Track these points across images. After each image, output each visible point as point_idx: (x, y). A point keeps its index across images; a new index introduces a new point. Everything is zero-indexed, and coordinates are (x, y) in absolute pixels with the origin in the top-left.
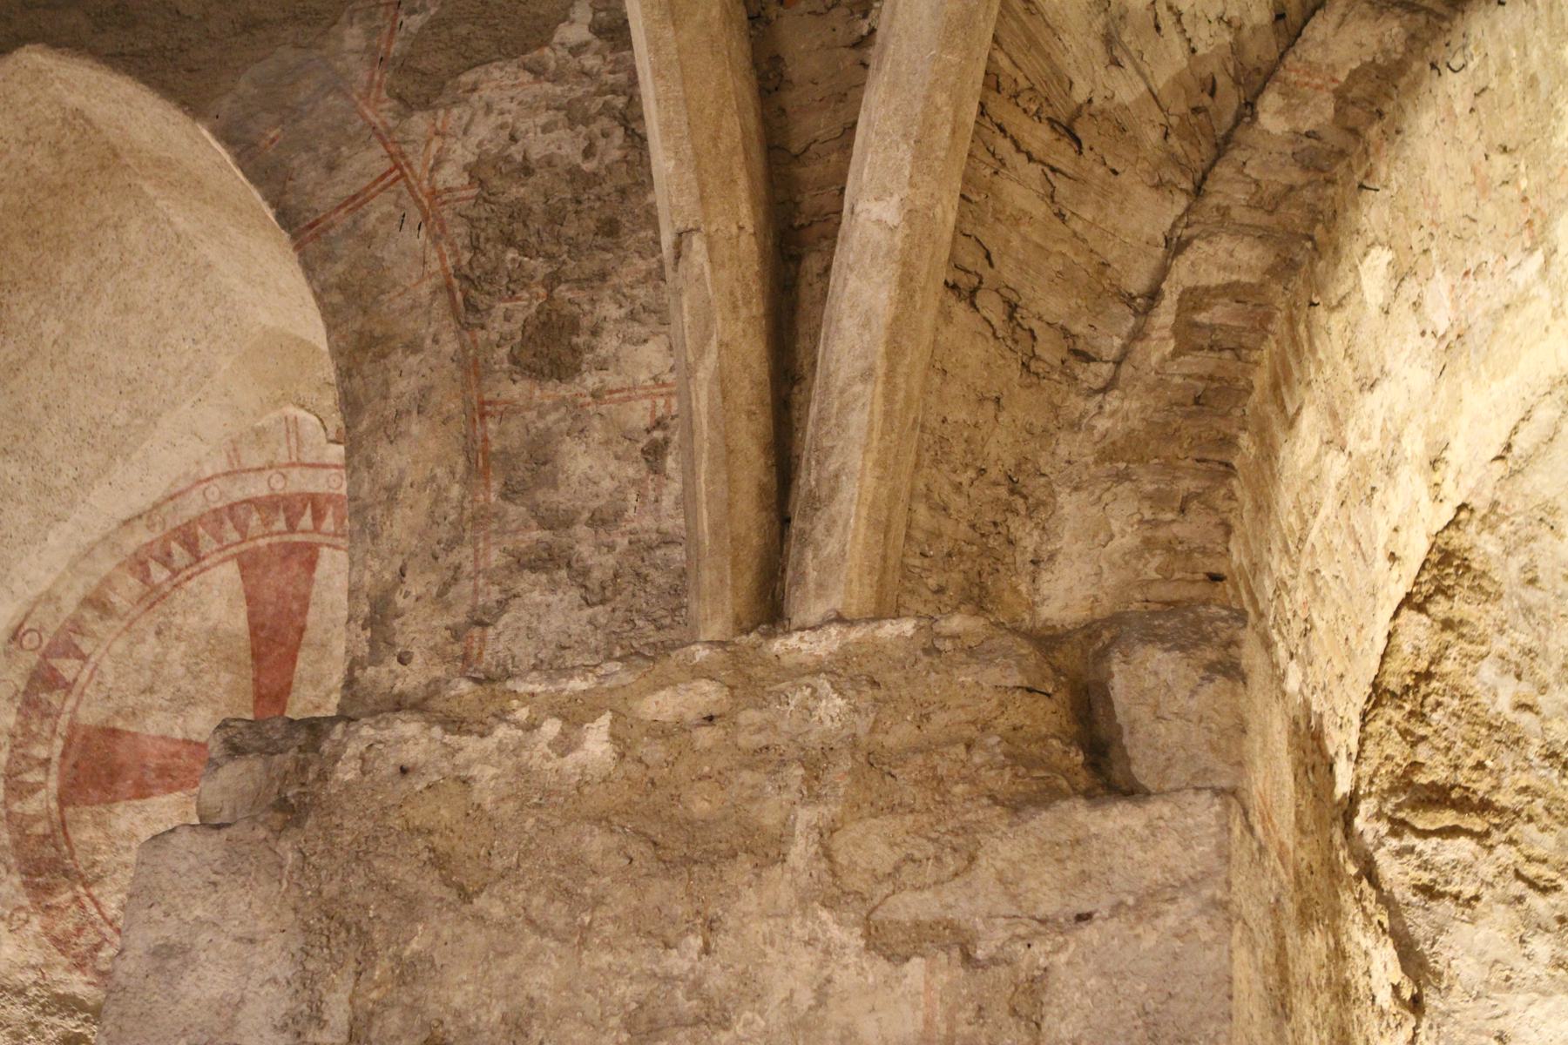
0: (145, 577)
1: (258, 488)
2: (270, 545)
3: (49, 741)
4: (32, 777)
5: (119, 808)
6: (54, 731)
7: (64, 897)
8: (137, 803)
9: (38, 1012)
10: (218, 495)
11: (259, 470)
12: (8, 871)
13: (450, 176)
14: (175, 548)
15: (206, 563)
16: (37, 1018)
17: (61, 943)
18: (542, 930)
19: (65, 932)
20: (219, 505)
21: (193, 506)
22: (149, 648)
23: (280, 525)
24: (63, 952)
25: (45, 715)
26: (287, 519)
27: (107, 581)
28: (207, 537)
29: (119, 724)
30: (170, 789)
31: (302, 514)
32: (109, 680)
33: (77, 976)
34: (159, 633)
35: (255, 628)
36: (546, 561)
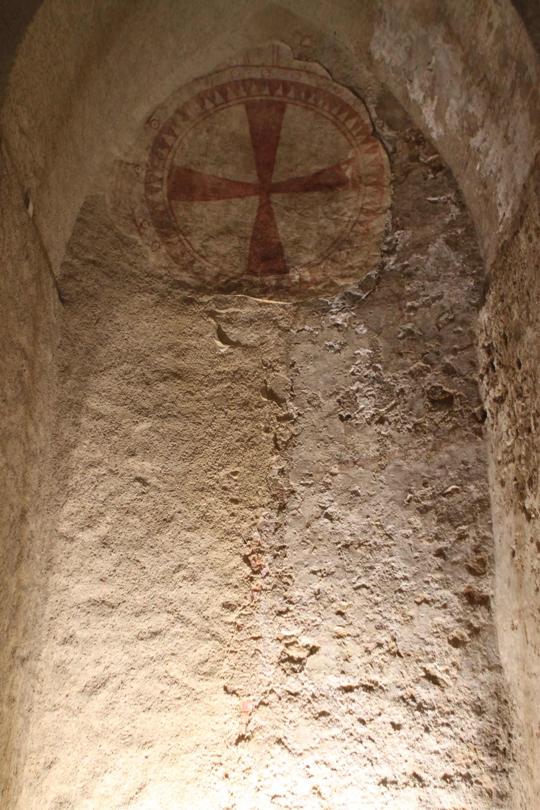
0: (203, 105)
1: (256, 74)
2: (261, 100)
3: (162, 171)
4: (156, 185)
5: (195, 204)
6: (164, 167)
7: (175, 239)
8: (203, 202)
9: (170, 287)
11: (258, 67)
12: (149, 225)
14: (217, 94)
15: (230, 103)
16: (170, 290)
17: (176, 259)
19: (176, 254)
20: (238, 79)
21: (226, 78)
22: (204, 137)
23: (266, 91)
24: (177, 263)
25: (160, 159)
26: (270, 90)
27: (186, 104)
28: (231, 92)
29: (193, 168)
30: (219, 199)
31: (278, 88)
32: (187, 147)
33: (184, 273)
34: (208, 131)
35: (253, 134)
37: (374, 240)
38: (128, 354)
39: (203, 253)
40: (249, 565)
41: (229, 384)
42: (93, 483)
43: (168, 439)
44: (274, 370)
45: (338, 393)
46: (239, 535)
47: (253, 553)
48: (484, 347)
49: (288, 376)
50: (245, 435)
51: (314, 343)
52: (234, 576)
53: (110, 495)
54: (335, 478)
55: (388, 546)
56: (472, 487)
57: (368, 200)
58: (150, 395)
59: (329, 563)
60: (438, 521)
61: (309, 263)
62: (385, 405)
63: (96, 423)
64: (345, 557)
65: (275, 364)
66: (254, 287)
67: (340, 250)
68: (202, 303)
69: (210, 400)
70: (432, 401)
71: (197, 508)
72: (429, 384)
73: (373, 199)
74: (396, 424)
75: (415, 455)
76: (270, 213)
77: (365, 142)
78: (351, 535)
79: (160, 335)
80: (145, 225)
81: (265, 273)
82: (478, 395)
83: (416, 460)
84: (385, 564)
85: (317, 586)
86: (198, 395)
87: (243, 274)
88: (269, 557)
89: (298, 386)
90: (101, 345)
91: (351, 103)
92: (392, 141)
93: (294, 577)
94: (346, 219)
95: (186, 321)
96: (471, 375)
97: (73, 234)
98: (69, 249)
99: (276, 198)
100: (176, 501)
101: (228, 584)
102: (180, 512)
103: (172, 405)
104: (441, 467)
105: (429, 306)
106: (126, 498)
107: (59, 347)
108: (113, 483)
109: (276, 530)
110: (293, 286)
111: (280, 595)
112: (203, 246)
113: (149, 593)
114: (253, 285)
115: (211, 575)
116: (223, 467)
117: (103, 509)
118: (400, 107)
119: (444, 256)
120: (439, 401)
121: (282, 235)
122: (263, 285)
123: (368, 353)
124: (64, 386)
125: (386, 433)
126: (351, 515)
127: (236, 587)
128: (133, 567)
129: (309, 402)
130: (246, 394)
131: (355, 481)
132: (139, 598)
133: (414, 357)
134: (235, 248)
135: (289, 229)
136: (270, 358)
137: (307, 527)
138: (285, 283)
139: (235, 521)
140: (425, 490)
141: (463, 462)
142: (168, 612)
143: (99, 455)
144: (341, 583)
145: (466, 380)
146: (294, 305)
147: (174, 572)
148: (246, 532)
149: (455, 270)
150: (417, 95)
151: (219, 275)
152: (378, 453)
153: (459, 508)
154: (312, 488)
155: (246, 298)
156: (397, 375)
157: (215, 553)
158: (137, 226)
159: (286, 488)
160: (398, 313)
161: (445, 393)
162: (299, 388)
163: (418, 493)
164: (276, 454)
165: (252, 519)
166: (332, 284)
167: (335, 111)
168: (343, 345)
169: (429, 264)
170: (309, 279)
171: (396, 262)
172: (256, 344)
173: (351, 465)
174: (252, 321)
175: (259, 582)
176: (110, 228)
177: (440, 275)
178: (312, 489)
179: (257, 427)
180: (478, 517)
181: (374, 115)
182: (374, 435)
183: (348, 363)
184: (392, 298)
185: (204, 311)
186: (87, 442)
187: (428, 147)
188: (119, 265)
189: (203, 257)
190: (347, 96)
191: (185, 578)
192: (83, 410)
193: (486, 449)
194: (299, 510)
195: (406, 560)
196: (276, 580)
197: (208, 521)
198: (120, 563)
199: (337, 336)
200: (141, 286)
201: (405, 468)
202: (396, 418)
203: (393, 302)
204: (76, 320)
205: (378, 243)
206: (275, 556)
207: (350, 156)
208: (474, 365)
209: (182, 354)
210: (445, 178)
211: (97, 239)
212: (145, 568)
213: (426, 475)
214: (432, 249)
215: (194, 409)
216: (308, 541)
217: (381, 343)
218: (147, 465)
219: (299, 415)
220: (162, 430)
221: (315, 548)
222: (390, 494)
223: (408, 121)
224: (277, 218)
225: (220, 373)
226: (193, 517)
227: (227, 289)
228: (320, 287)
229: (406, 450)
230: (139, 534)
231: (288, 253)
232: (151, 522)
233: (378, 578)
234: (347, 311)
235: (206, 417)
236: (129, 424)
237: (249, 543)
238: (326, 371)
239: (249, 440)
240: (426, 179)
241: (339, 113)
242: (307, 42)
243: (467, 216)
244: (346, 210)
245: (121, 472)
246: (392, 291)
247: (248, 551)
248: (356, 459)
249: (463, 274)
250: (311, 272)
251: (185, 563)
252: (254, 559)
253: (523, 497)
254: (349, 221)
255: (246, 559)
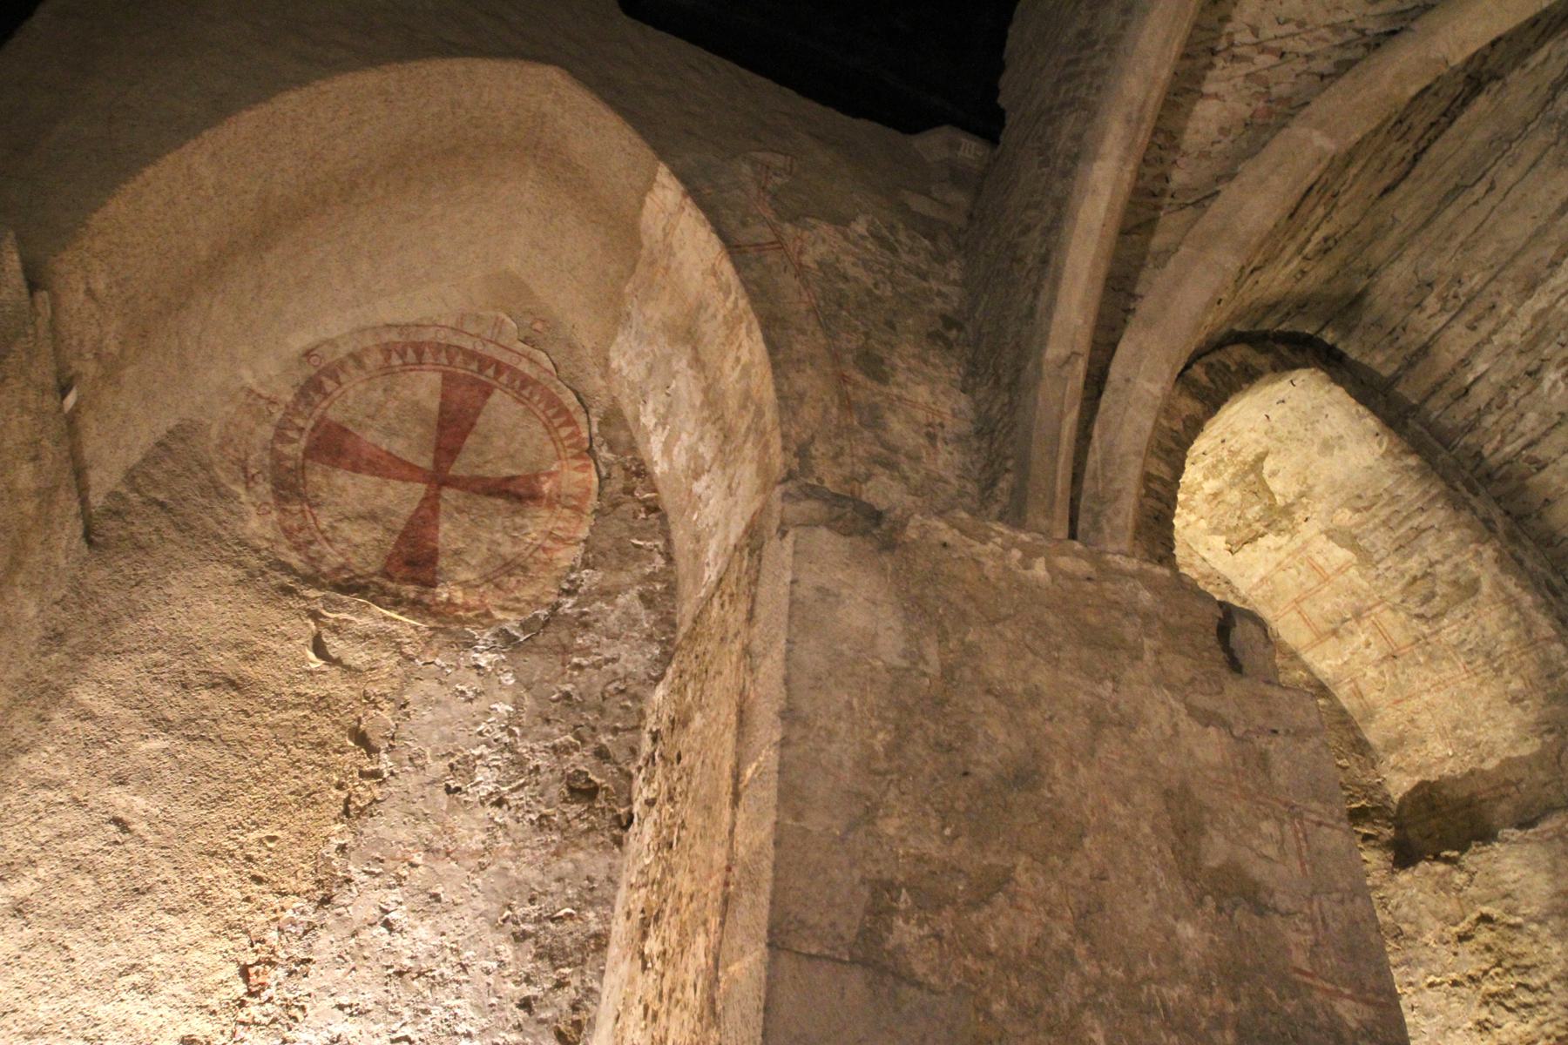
0: (388, 358)
1: (468, 344)
2: (464, 375)
3: (307, 419)
4: (292, 434)
6: (311, 415)
10: (442, 336)
13: (807, 259)
14: (410, 352)
16: (265, 569)
17: (288, 533)
18: (1036, 654)
19: (291, 527)
21: (428, 335)
22: (377, 395)
23: (474, 366)
24: (288, 538)
25: (309, 404)
27: (366, 349)
29: (350, 427)
30: (373, 474)
31: (489, 367)
32: (350, 402)
35: (442, 412)
36: (890, 465)
37: (554, 574)
38: (170, 640)
39: (329, 535)
40: (247, 979)
41: (307, 712)
42: (36, 812)
43: (187, 771)
44: (376, 707)
45: (453, 755)
46: (247, 932)
47: (258, 963)
48: (651, 732)
49: (393, 719)
50: (306, 787)
51: (441, 683)
52: (216, 995)
53: (60, 836)
54: (415, 871)
55: (457, 982)
56: (591, 915)
57: (561, 524)
58: (182, 703)
59: (367, 996)
60: (535, 956)
61: (467, 581)
62: (509, 783)
63: (78, 723)
64: (392, 989)
65: (380, 699)
66: (384, 594)
67: (510, 575)
68: (305, 598)
69: (271, 728)
70: (572, 790)
71: (196, 880)
72: (573, 766)
73: (567, 525)
74: (517, 811)
75: (530, 858)
76: (435, 510)
77: (575, 457)
78: (412, 958)
79: (228, 625)
80: (260, 478)
81: (404, 580)
82: (630, 793)
83: (530, 864)
84: (447, 1008)
85: (336, 1030)
86: (257, 719)
87: (374, 574)
88: (281, 973)
89: (403, 734)
90: (131, 616)
91: (572, 409)
92: (608, 465)
93: (308, 1010)
94: (529, 540)
95: (273, 614)
96: (628, 764)
97: (144, 460)
98: (130, 477)
99: (448, 494)
100: (166, 864)
101: (201, 1007)
102: (165, 882)
103: (212, 723)
104: (559, 880)
105: (599, 667)
106: (85, 845)
107: (57, 603)
108: (73, 819)
109: (305, 933)
110: (437, 605)
111: (277, 1034)
112: (333, 527)
113: (65, 1002)
114: (383, 591)
115: (180, 988)
116: (258, 827)
117: (38, 855)
118: (626, 428)
119: (633, 611)
120: (580, 791)
121: (441, 539)
122: (397, 595)
123: (508, 711)
124: (43, 659)
125: (500, 821)
126: (420, 928)
127: (214, 1013)
128: (53, 956)
129: (411, 759)
130: (326, 731)
131: (441, 879)
132: (44, 1009)
133: (564, 727)
134: (375, 539)
135: (453, 534)
136: (376, 690)
137: (353, 936)
138: (427, 599)
139: (247, 909)
140: (530, 908)
141: (588, 878)
142: (85, 1039)
143: (65, 772)
144: (375, 1028)
145: (620, 770)
146: (431, 629)
147: (120, 975)
148: (258, 929)
149: (642, 631)
150: (648, 420)
151: (342, 567)
152: (482, 846)
153: (568, 941)
154: (377, 879)
155: (368, 606)
156: (536, 747)
157: (199, 953)
158: (246, 476)
159: (340, 874)
160: (559, 668)
161: (590, 781)
162: (403, 738)
163: (520, 912)
164: (342, 821)
165: (275, 911)
166: (488, 614)
167: (550, 413)
168: (478, 694)
169: (613, 617)
170: (459, 601)
171: (574, 606)
172: (363, 668)
173: (442, 855)
174: (367, 637)
175: (254, 1010)
176: (205, 467)
177: (622, 634)
178: (377, 881)
179: (327, 780)
180: (589, 959)
181: (595, 430)
182: (483, 820)
183: (478, 717)
184: (558, 649)
185: (304, 609)
186: (51, 749)
187: (647, 482)
188: (199, 519)
189: (327, 540)
190: (570, 400)
191: (134, 987)
192: (64, 702)
193: (622, 865)
194: (350, 908)
195: (477, 1006)
196: (279, 1010)
197: (205, 903)
198: (34, 946)
199: (473, 683)
200: (225, 554)
201: (513, 873)
202: (520, 802)
203: (557, 653)
204: (104, 573)
205: (558, 579)
206: (291, 973)
207: (554, 468)
208: (634, 752)
209: (252, 658)
210: (658, 522)
211: (179, 476)
212: (73, 960)
213: (537, 888)
214: (621, 600)
215: (244, 736)
216: (348, 957)
217: (528, 701)
218: (140, 802)
219: (392, 774)
220: (182, 756)
221: (354, 969)
222: (483, 907)
223: (632, 447)
224: (442, 518)
225: (298, 695)
226: (184, 892)
227: (348, 588)
228: (470, 614)
229: (521, 849)
230: (85, 904)
231: (443, 563)
232: (113, 889)
233: (431, 1029)
234: (496, 652)
235: (257, 751)
236: (133, 738)
237: (257, 946)
238: (447, 723)
239: (309, 796)
240: (635, 517)
241: (555, 416)
242: (538, 326)
243: (672, 572)
244: (530, 529)
245: (92, 804)
246: (559, 639)
247: (250, 958)
248: (451, 848)
249: (650, 638)
250: (465, 594)
251: (144, 962)
252: (257, 973)
253: (645, 936)
254: (531, 544)
255: (244, 972)
